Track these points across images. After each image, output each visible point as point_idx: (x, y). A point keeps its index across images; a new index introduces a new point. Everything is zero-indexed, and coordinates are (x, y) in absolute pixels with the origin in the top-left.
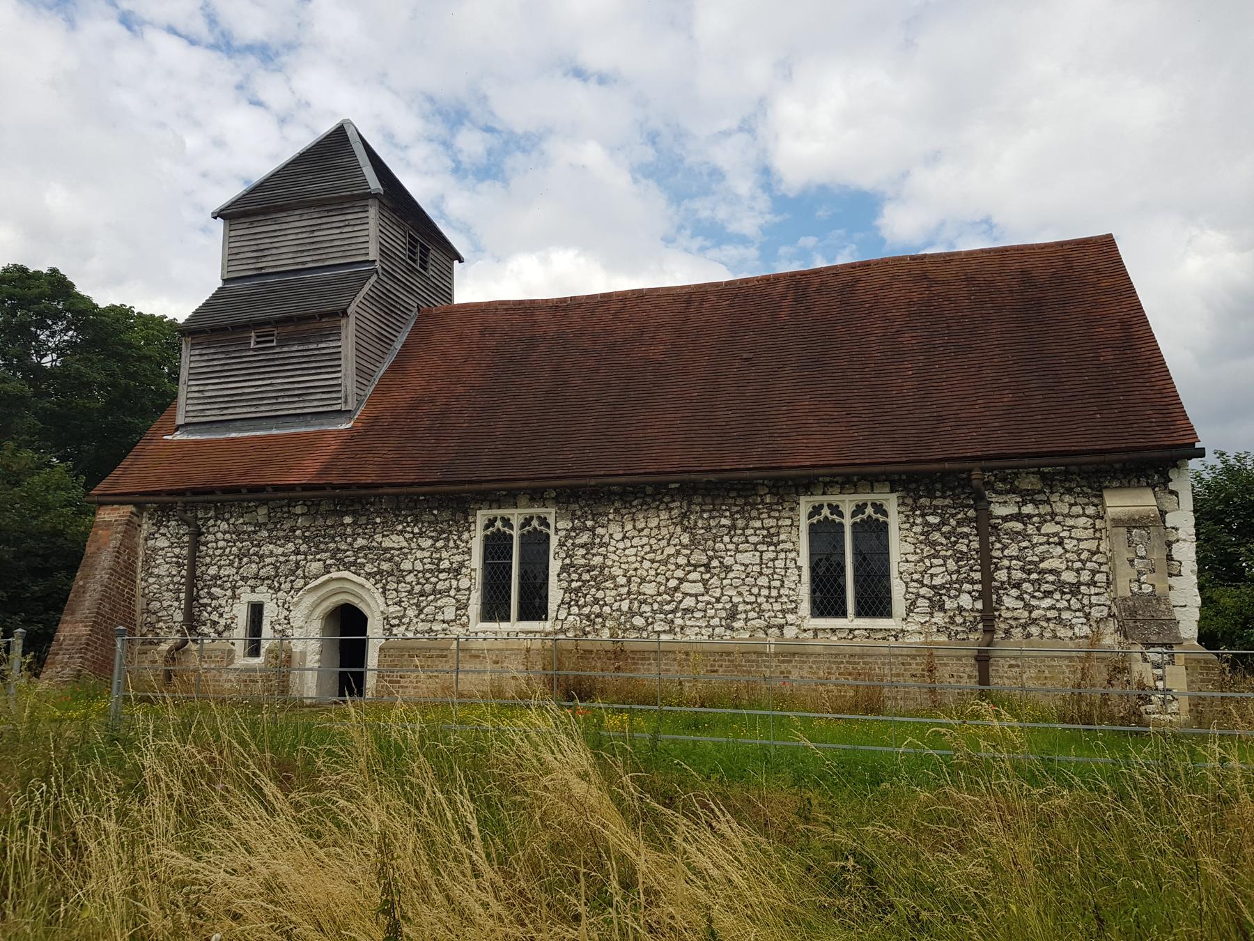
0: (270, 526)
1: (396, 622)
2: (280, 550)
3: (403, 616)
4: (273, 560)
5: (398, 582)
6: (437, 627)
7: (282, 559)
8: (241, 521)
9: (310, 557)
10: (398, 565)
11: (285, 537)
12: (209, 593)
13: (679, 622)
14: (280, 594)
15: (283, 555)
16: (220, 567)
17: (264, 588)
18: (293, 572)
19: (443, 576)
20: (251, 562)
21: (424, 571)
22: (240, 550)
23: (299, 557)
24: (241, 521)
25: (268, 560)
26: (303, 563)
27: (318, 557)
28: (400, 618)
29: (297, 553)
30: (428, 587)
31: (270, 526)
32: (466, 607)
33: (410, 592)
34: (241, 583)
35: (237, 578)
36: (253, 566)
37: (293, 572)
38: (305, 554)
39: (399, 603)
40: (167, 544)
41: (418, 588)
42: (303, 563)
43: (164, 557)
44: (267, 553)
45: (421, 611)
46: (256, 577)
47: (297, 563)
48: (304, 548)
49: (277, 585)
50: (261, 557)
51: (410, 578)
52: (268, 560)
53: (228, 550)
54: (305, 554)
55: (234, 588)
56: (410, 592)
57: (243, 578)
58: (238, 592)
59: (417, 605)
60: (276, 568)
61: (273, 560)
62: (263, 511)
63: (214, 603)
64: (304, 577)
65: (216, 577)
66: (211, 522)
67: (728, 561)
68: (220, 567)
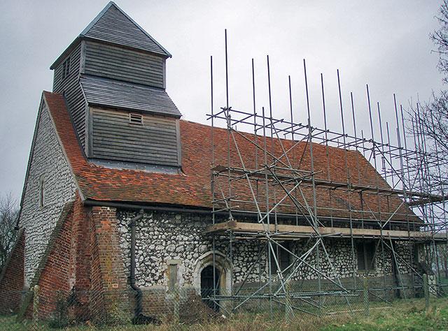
0: (181, 226)
1: (238, 274)
2: (186, 238)
3: (241, 271)
4: (183, 243)
5: (238, 256)
6: (254, 276)
7: (187, 243)
8: (167, 221)
9: (200, 243)
10: (238, 248)
11: (189, 231)
12: (150, 259)
13: (328, 272)
14: (187, 261)
15: (188, 241)
16: (156, 245)
17: (178, 258)
18: (193, 250)
19: (255, 254)
20: (171, 244)
21: (249, 251)
22: (166, 236)
23: (196, 242)
24: (167, 221)
25: (181, 243)
26: (197, 245)
27: (204, 243)
28: (240, 272)
29: (195, 240)
30: (250, 259)
31: (181, 226)
32: (264, 267)
33: (243, 261)
34: (166, 254)
35: (165, 251)
36: (173, 245)
37: (193, 250)
38: (198, 241)
39: (239, 266)
40: (127, 231)
41: (246, 259)
42: (197, 245)
43: (126, 238)
44: (180, 239)
45: (248, 270)
46: (175, 251)
47: (195, 245)
48: (197, 238)
49: (185, 256)
50: (177, 241)
51: (243, 254)
52: (181, 243)
53: (160, 236)
54: (198, 241)
55: (163, 257)
56: (243, 261)
57: (168, 252)
58: (165, 259)
59: (246, 266)
60: (185, 247)
61: (183, 243)
62: (178, 217)
63: (153, 264)
64: (198, 252)
65: (152, 251)
66: (151, 221)
67: (340, 251)
68: (156, 245)
